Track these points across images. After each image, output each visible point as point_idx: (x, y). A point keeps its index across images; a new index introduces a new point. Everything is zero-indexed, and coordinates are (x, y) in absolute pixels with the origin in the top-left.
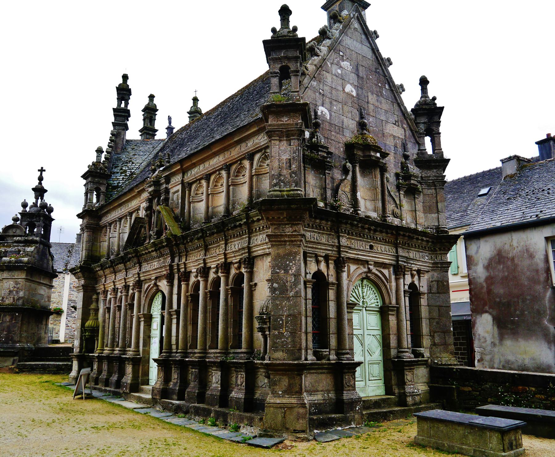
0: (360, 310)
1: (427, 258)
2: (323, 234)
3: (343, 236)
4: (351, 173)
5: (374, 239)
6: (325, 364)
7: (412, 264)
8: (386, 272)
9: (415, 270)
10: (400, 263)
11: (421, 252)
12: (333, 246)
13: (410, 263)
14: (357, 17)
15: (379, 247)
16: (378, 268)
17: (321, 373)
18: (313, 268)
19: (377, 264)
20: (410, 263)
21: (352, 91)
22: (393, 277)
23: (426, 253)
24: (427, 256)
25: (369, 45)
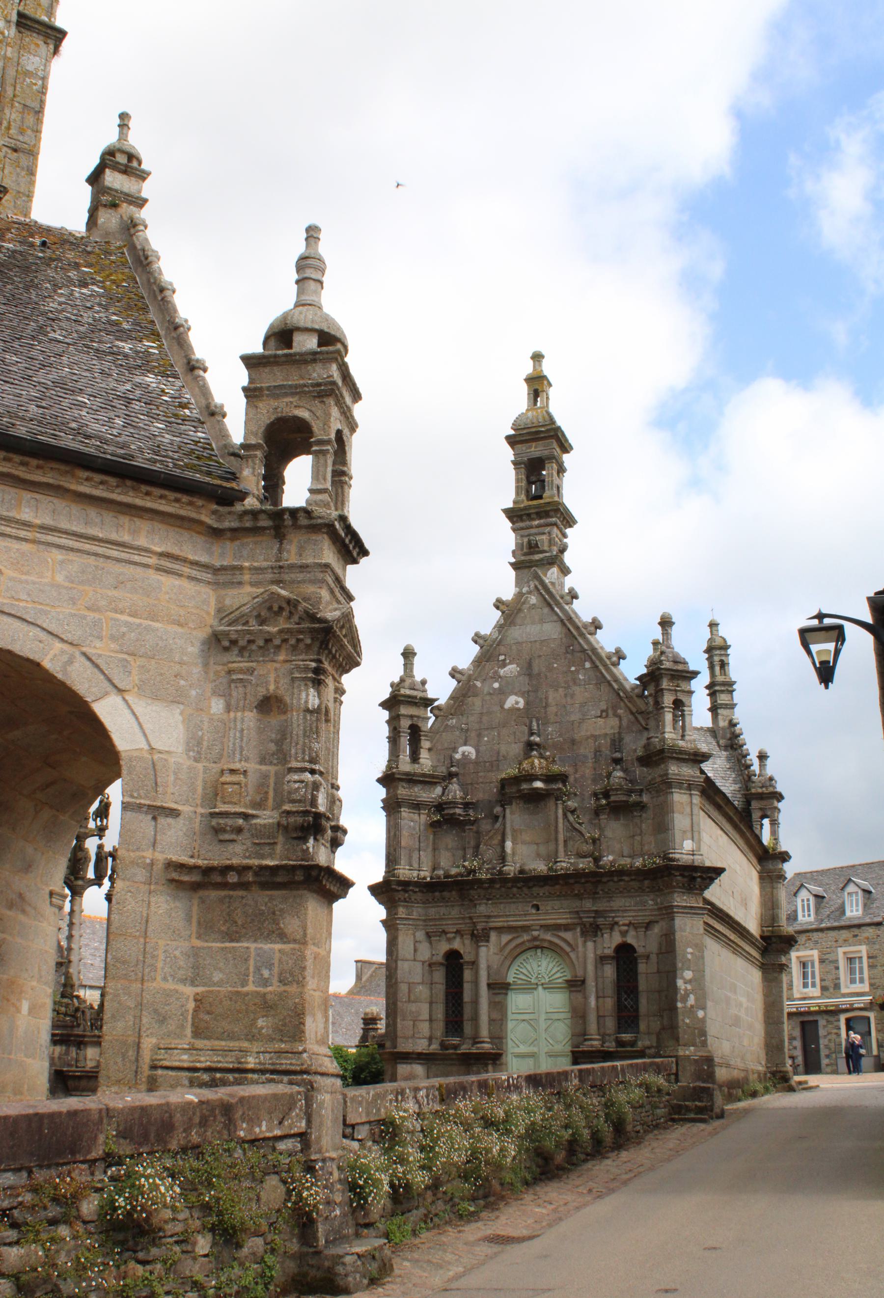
0: (535, 989)
1: (651, 902)
2: (453, 906)
3: (480, 904)
4: (500, 819)
5: (536, 897)
6: (453, 1054)
7: (613, 917)
8: (568, 936)
9: (624, 925)
10: (584, 920)
11: (639, 896)
12: (463, 918)
13: (609, 917)
14: (536, 587)
15: (547, 906)
16: (555, 932)
17: (451, 1065)
18: (444, 947)
19: (546, 928)
20: (609, 917)
21: (517, 703)
22: (580, 941)
23: (648, 896)
24: (652, 900)
25: (555, 618)
